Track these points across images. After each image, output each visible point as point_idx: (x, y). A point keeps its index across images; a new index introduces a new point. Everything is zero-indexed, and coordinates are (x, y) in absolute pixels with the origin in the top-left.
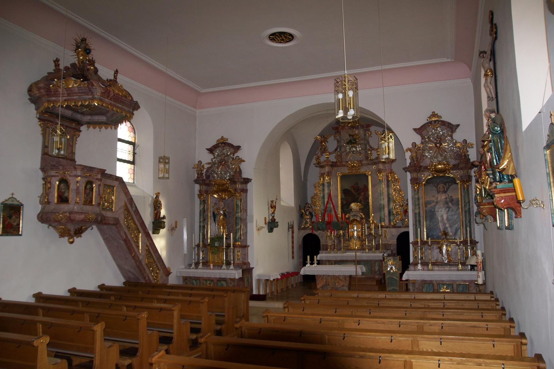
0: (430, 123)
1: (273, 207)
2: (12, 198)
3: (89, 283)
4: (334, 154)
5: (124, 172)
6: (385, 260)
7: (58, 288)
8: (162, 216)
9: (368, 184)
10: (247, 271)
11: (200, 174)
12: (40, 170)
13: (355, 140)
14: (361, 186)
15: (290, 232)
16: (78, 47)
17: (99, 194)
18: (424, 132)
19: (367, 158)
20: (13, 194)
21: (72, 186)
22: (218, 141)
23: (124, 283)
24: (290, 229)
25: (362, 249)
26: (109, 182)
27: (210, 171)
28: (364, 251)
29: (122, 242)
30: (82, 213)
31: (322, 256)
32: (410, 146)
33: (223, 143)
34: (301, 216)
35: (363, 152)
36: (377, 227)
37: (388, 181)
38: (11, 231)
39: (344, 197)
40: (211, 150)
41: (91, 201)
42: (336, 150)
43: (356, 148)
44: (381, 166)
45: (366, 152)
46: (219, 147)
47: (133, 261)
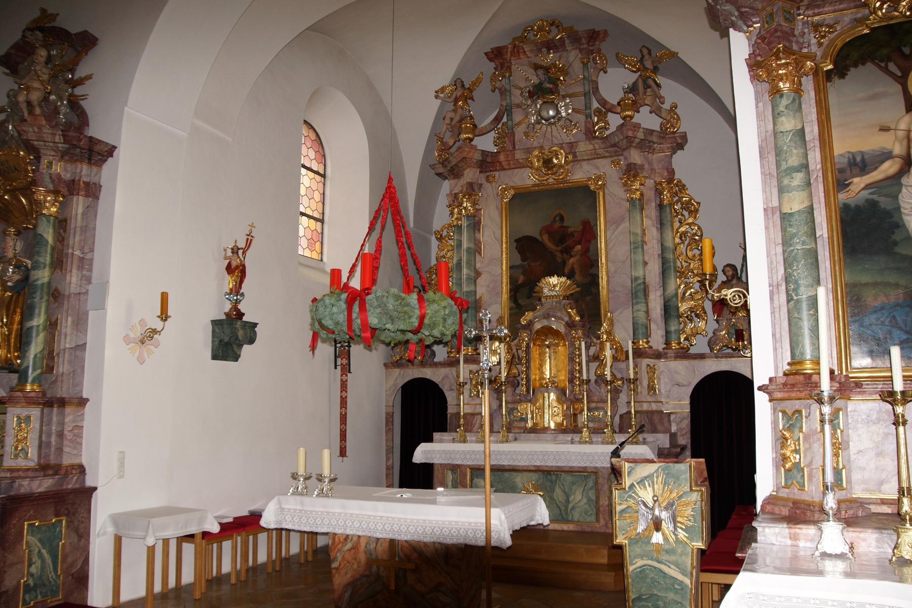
1: (237, 271)
4: (493, 134)
6: (627, 481)
9: (596, 219)
13: (555, 81)
14: (573, 223)
19: (590, 134)
25: (570, 428)
28: (577, 437)
35: (581, 118)
36: (620, 355)
39: (518, 261)
42: (498, 119)
44: (635, 157)
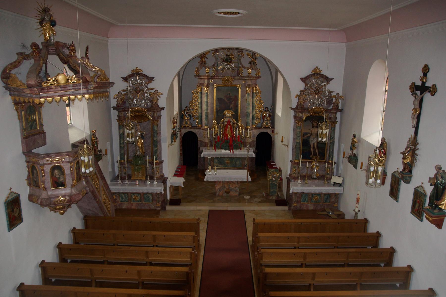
0: (314, 74)
2: (11, 192)
8: (99, 149)
10: (164, 180)
12: (23, 154)
18: (308, 81)
20: (11, 189)
21: (67, 171)
22: (133, 71)
33: (137, 73)
38: (16, 222)
40: (125, 79)
42: (214, 65)
43: (231, 65)
45: (238, 70)
47: (97, 204)
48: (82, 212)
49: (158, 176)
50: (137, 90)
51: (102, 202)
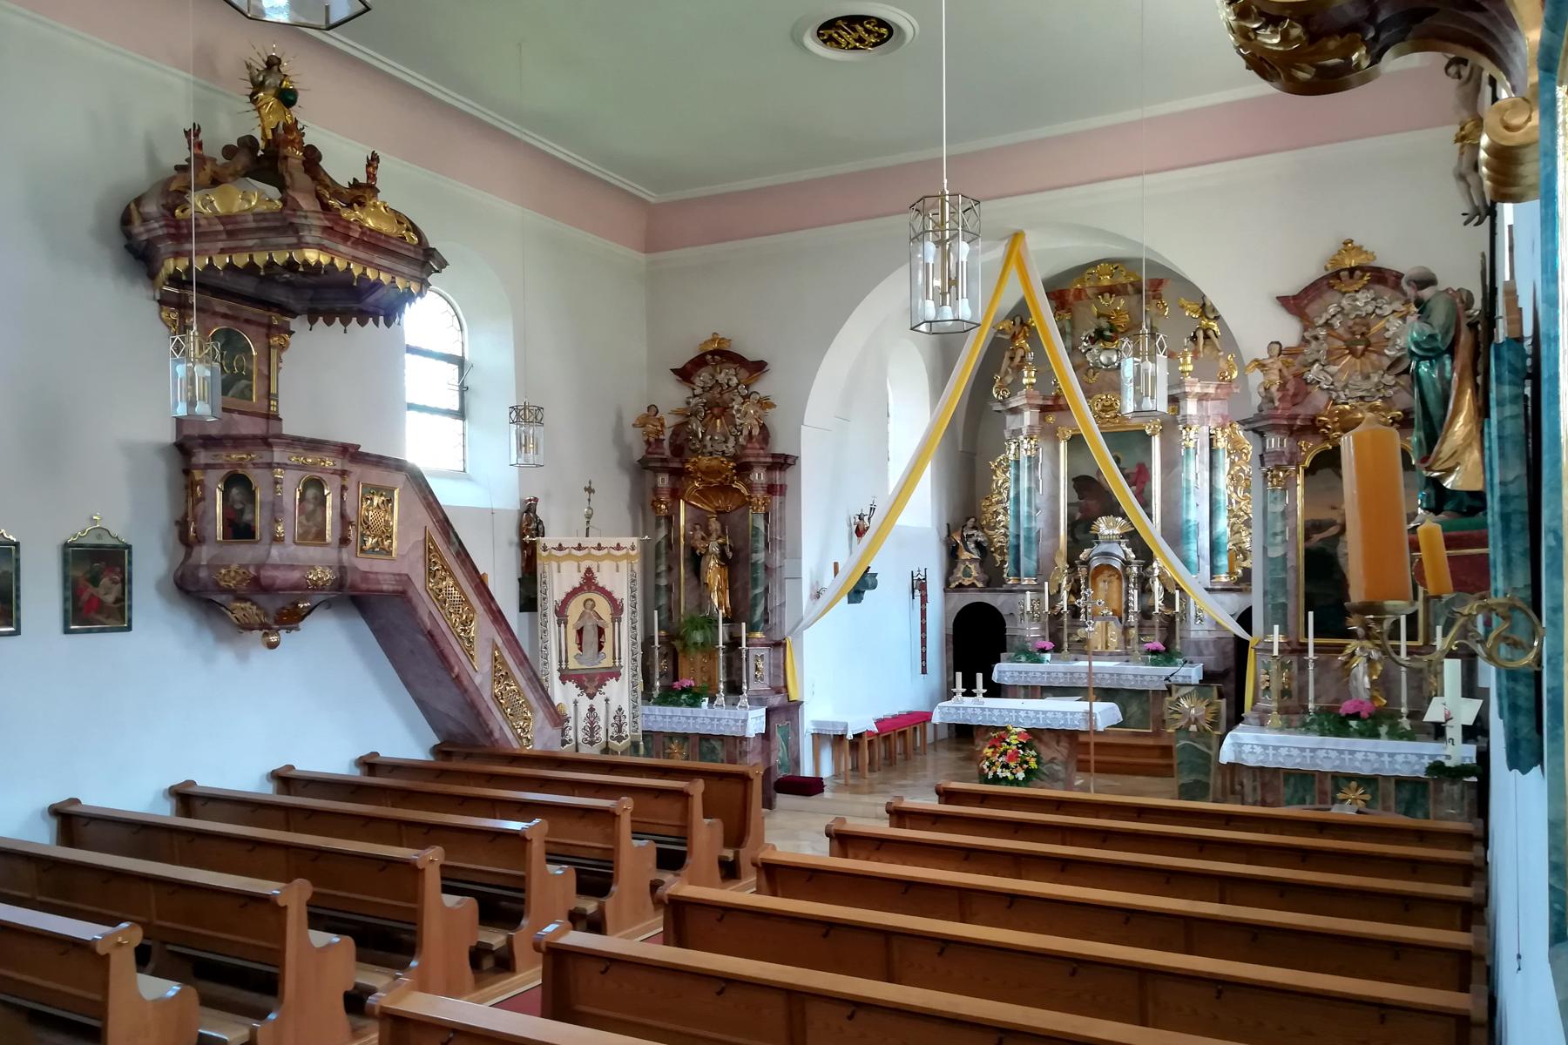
0: (1336, 275)
3: (333, 758)
5: (428, 445)
7: (242, 772)
10: (784, 711)
11: (653, 444)
15: (918, 599)
16: (258, 86)
17: (343, 516)
18: (1312, 309)
23: (437, 751)
24: (917, 592)
26: (375, 476)
27: (683, 435)
29: (422, 639)
30: (292, 567)
31: (1004, 671)
32: (1263, 355)
34: (952, 554)
37: (1213, 451)
39: (1076, 499)
40: (684, 375)
41: (321, 535)
46: (706, 363)
48: (436, 730)
49: (762, 686)
50: (717, 408)
51: (487, 695)
